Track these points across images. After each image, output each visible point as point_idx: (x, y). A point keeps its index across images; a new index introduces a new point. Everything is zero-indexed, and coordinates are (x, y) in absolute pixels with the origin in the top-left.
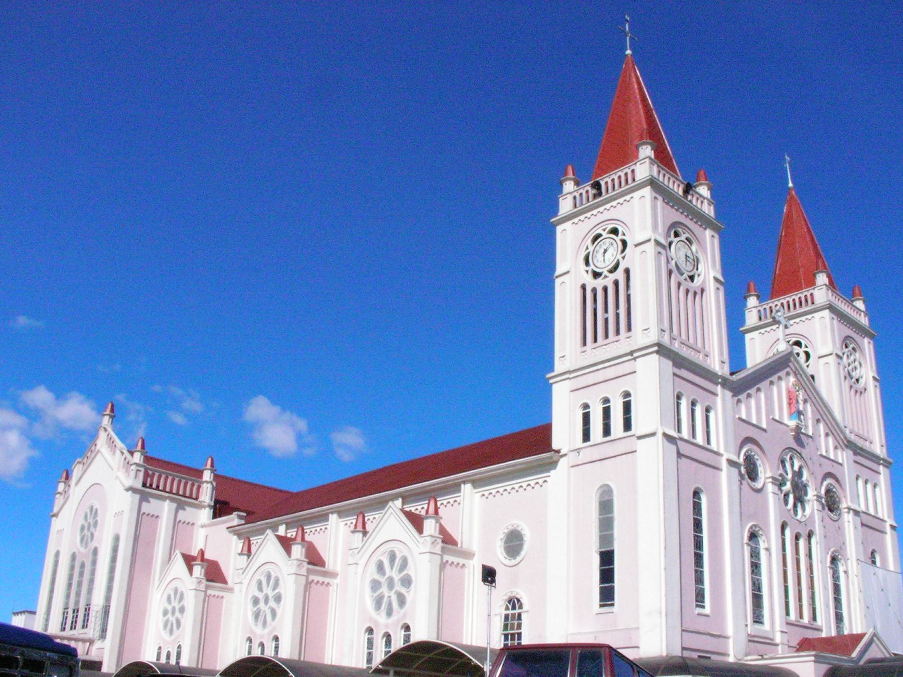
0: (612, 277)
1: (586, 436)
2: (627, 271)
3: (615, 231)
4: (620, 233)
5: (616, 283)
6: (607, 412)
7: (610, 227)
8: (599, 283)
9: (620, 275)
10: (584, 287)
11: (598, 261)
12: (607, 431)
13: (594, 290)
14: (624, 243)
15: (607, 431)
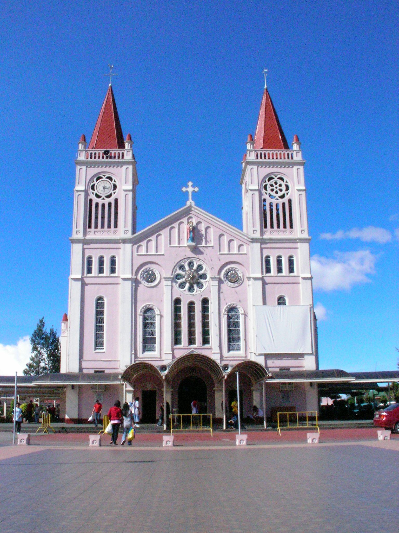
0: (107, 201)
1: (90, 271)
2: (116, 201)
3: (110, 178)
4: (113, 180)
5: (110, 204)
6: (101, 262)
7: (107, 176)
8: (100, 201)
9: (112, 200)
10: (91, 200)
11: (99, 190)
12: (101, 270)
13: (97, 204)
14: (115, 187)
15: (101, 270)
